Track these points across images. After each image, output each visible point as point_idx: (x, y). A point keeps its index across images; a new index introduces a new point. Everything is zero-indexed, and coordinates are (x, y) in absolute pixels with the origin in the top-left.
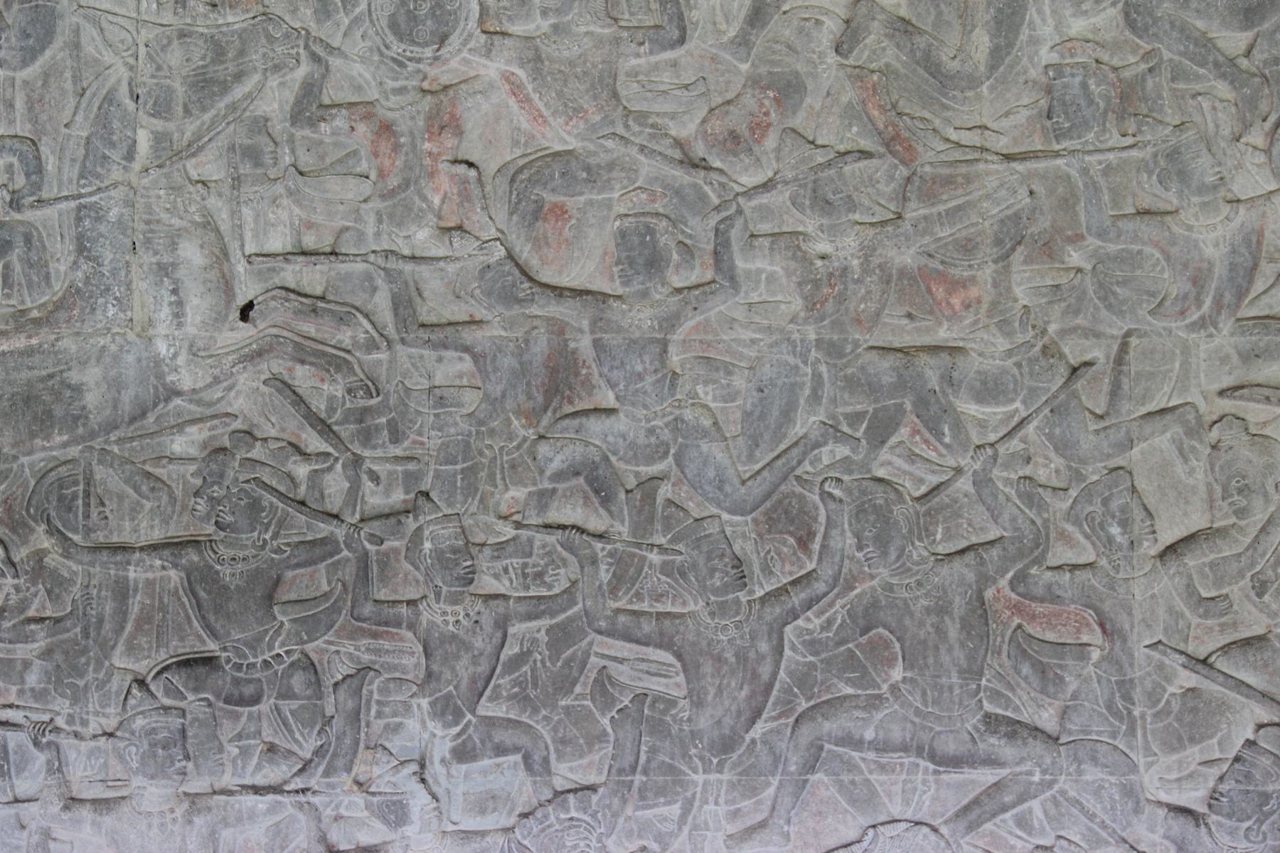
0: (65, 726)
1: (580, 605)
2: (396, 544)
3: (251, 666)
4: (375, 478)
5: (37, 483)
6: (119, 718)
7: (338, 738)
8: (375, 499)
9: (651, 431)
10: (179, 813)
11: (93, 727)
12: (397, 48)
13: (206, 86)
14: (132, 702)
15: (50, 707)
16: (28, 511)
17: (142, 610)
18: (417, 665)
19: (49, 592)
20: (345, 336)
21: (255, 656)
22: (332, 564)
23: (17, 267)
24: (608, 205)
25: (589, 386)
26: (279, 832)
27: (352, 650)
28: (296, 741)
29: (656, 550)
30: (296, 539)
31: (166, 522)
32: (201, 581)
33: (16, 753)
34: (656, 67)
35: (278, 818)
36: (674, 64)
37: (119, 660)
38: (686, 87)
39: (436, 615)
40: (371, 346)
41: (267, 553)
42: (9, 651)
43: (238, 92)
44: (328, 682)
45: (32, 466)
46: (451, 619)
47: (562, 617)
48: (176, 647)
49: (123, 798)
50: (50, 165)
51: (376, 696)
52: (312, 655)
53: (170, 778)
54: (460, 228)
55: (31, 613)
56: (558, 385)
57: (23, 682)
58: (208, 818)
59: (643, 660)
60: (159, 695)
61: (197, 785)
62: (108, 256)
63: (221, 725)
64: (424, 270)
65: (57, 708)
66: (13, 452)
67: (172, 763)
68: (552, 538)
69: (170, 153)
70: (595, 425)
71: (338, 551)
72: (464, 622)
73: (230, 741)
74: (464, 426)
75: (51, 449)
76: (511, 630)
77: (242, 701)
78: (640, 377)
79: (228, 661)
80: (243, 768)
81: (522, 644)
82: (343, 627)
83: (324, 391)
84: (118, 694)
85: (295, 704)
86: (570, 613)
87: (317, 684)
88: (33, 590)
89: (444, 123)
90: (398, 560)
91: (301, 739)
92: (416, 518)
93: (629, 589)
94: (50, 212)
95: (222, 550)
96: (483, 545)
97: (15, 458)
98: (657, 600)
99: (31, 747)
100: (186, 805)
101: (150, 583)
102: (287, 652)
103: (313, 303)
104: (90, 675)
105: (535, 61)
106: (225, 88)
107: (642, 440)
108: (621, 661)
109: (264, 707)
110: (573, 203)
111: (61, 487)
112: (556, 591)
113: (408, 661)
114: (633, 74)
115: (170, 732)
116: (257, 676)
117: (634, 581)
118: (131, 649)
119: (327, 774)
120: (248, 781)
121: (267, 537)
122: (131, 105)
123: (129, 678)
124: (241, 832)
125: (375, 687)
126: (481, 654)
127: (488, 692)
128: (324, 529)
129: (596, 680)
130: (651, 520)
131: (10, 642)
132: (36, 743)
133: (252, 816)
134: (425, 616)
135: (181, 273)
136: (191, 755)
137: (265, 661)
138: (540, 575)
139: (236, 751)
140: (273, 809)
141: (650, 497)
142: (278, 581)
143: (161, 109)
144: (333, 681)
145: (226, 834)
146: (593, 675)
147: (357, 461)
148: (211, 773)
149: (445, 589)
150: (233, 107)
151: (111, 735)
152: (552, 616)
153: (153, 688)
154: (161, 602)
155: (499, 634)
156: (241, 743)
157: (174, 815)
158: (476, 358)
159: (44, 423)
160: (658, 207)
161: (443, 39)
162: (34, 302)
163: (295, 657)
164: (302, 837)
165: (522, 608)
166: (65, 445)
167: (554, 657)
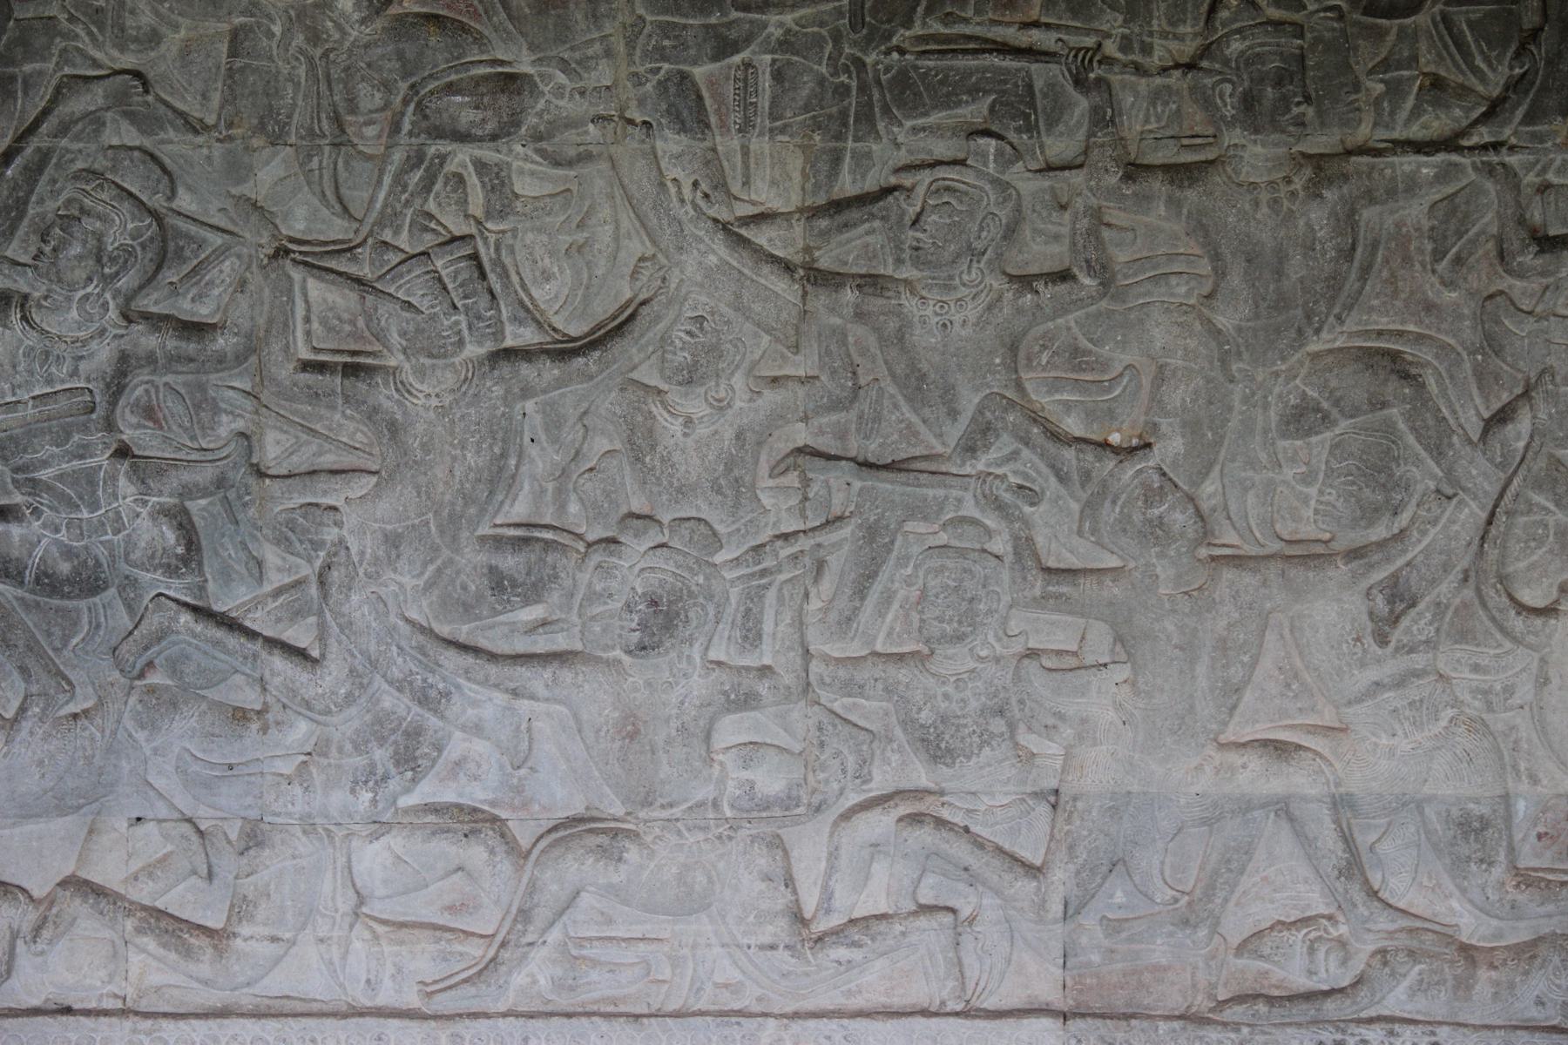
0: (1119, 55)
6: (1199, 41)
7: (1549, 62)
10: (1298, 184)
11: (1157, 58)
15: (1096, 25)
26: (1454, 211)
28: (1475, 70)
33: (1045, 96)
35: (1450, 190)
49: (1211, 162)
53: (1283, 132)
58: (1345, 190)
61: (1320, 142)
63: (1356, 49)
65: (1105, 27)
67: (1289, 110)
73: (1371, 72)
80: (1392, 113)
91: (1483, 66)
99: (1070, 88)
100: (1308, 172)
115: (1283, 60)
119: (1529, 119)
120: (1396, 135)
124: (1392, 212)
132: (1079, 82)
133: (1412, 186)
136: (1313, 95)
139: (1380, 87)
140: (1444, 175)
145: (1368, 214)
148: (1345, 123)
151: (1190, 66)
156: (1387, 76)
157: (1292, 187)
164: (1490, 215)
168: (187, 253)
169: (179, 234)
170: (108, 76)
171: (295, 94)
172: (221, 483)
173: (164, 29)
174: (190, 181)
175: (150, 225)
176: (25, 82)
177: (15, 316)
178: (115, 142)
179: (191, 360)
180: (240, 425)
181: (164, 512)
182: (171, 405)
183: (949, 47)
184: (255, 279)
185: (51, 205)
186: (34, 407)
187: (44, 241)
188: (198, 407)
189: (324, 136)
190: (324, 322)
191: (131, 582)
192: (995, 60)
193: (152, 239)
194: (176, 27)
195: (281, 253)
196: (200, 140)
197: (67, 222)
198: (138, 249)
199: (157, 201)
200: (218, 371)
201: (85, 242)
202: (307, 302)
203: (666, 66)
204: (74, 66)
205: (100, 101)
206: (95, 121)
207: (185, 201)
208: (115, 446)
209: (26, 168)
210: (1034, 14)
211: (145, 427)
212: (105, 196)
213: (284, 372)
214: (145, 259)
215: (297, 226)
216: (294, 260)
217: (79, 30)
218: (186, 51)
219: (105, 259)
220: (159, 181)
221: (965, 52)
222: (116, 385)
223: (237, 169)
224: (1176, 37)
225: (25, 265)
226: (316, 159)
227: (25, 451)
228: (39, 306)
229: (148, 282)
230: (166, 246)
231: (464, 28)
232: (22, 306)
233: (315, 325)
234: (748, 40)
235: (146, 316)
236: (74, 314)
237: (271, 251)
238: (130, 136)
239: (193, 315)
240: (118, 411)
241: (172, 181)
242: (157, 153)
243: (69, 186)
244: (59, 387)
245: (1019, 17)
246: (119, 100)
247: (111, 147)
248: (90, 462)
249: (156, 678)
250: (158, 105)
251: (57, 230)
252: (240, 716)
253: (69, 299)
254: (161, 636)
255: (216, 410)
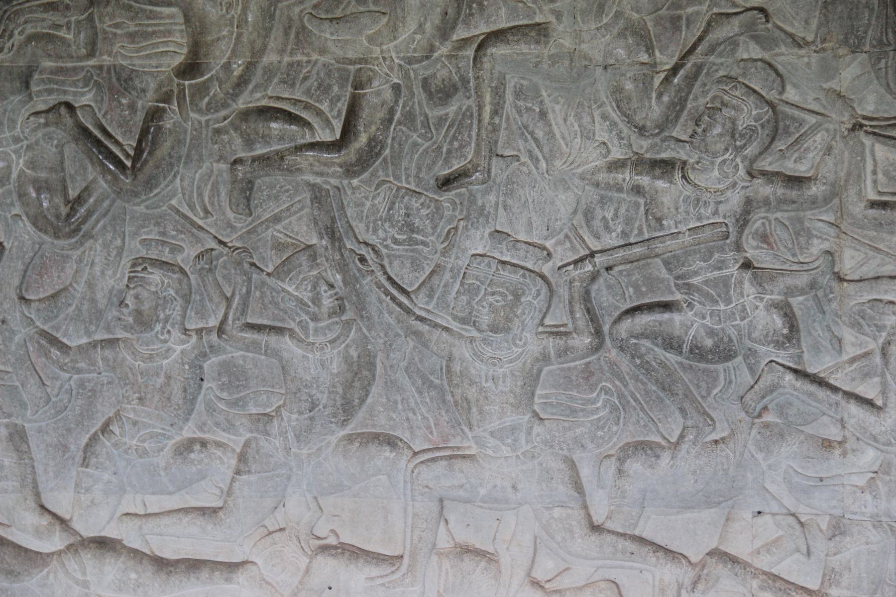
168: (792, 129)
169: (787, 116)
170: (742, 12)
171: (870, 16)
172: (813, 285)
174: (795, 81)
175: (767, 111)
176: (688, 20)
177: (678, 175)
178: (745, 56)
179: (794, 202)
180: (826, 246)
181: (776, 305)
182: (779, 233)
184: (838, 145)
185: (702, 101)
186: (690, 236)
187: (697, 125)
188: (797, 234)
189: (890, 44)
190: (886, 173)
191: (752, 352)
193: (768, 121)
195: (857, 127)
196: (803, 52)
197: (713, 111)
198: (759, 128)
199: (772, 96)
200: (811, 209)
201: (724, 125)
202: (874, 160)
204: (720, 7)
205: (737, 30)
206: (733, 42)
207: (791, 94)
208: (741, 261)
209: (687, 77)
211: (762, 248)
212: (737, 93)
213: (858, 209)
214: (763, 134)
215: (869, 107)
216: (866, 132)
219: (737, 136)
220: (774, 81)
222: (743, 221)
223: (828, 71)
225: (684, 141)
226: (883, 61)
227: (683, 265)
228: (694, 169)
229: (765, 150)
230: (778, 126)
232: (682, 168)
233: (880, 176)
235: (764, 173)
236: (716, 173)
237: (850, 126)
238: (756, 52)
239: (795, 171)
240: (744, 238)
241: (783, 81)
242: (773, 62)
243: (715, 88)
244: (705, 222)
246: (749, 29)
247: (742, 60)
248: (726, 272)
249: (769, 418)
250: (775, 30)
251: (706, 118)
252: (827, 444)
253: (713, 163)
254: (773, 389)
255: (810, 236)
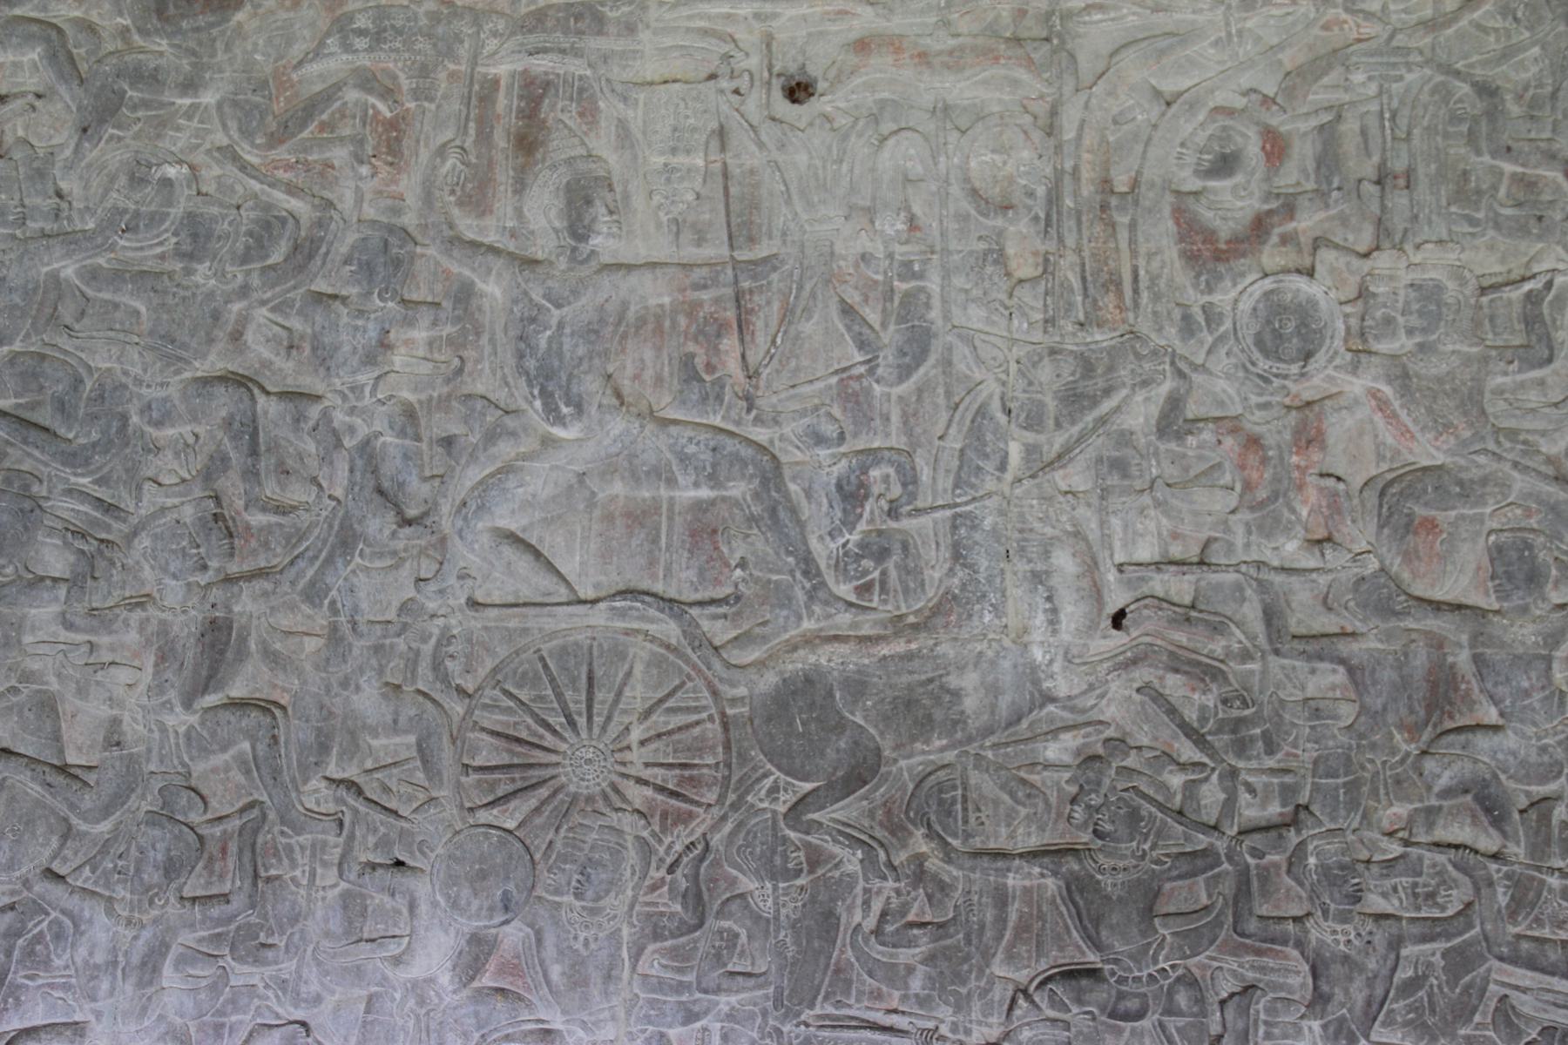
0: (949, 1035)
1: (1478, 929)
2: (1276, 858)
3: (1137, 979)
4: (1251, 790)
5: (917, 786)
6: (1002, 1029)
8: (1251, 811)
9: (1543, 749)
12: (1264, 364)
13: (1075, 400)
14: (1017, 1012)
16: (907, 812)
17: (1020, 918)
18: (1303, 985)
19: (930, 897)
20: (1218, 646)
21: (1140, 970)
22: (1213, 877)
23: (893, 574)
24: (1480, 519)
25: (1471, 704)
27: (1235, 966)
29: (1557, 874)
30: (1175, 850)
31: (1042, 829)
32: (1078, 889)
34: (1522, 385)
36: (1541, 382)
37: (998, 969)
38: (1556, 405)
39: (1321, 933)
40: (1246, 656)
41: (1147, 864)
42: (892, 956)
43: (1106, 406)
44: (1213, 1001)
45: (910, 769)
46: (1342, 938)
47: (1458, 940)
48: (1056, 958)
50: (925, 475)
51: (1262, 1016)
52: (1194, 970)
54: (1329, 539)
55: (911, 917)
56: (1439, 702)
57: (907, 987)
59: (1549, 991)
60: (1043, 1006)
62: (983, 564)
64: (1294, 580)
66: (894, 755)
68: (1441, 858)
69: (1040, 465)
70: (1483, 742)
71: (1219, 864)
72: (1356, 942)
74: (1343, 739)
75: (929, 753)
76: (1404, 952)
77: (1127, 1017)
78: (1527, 693)
79: (1113, 973)
81: (1416, 968)
82: (1225, 941)
83: (1196, 701)
84: (1001, 1004)
85: (1181, 1022)
86: (1467, 936)
87: (1200, 1001)
88: (913, 894)
89: (1309, 438)
90: (1278, 875)
92: (1299, 832)
93: (1529, 914)
94: (925, 521)
95: (1101, 858)
96: (1368, 862)
97: (895, 761)
98: (1560, 928)
101: (1027, 891)
102: (1172, 967)
103: (1187, 614)
104: (973, 984)
105: (1402, 377)
106: (1095, 402)
107: (1533, 758)
108: (1525, 990)
109: (1146, 1023)
110: (1444, 517)
111: (941, 791)
112: (1450, 913)
113: (1295, 981)
114: (1499, 392)
116: (1143, 990)
117: (1533, 905)
118: (1010, 958)
121: (1146, 847)
122: (1002, 418)
123: (1011, 987)
125: (1261, 1006)
126: (1375, 977)
127: (1381, 1017)
128: (1202, 840)
129: (1496, 1009)
130: (1548, 841)
131: (894, 946)
134: (1314, 934)
135: (1055, 581)
137: (1150, 975)
138: (1431, 896)
141: (1545, 818)
142: (1157, 893)
143: (1034, 422)
144: (1217, 999)
146: (1493, 1004)
147: (1233, 773)
149: (1333, 906)
150: (1102, 421)
152: (1448, 939)
153: (1037, 999)
154: (1040, 910)
155: (1393, 956)
158: (1351, 671)
159: (926, 727)
160: (1533, 522)
161: (1308, 356)
162: (912, 607)
163: (1180, 972)
165: (1416, 930)
166: (942, 749)
167: (1453, 983)
173: (324, 994)
183: (838, 1024)
192: (868, 1034)
194: (333, 993)
203: (651, 1028)
210: (895, 1004)
217: (270, 993)
218: (337, 1009)
221: (849, 1027)
224: (987, 1025)
231: (520, 998)
234: (706, 1013)
245: (884, 1006)
